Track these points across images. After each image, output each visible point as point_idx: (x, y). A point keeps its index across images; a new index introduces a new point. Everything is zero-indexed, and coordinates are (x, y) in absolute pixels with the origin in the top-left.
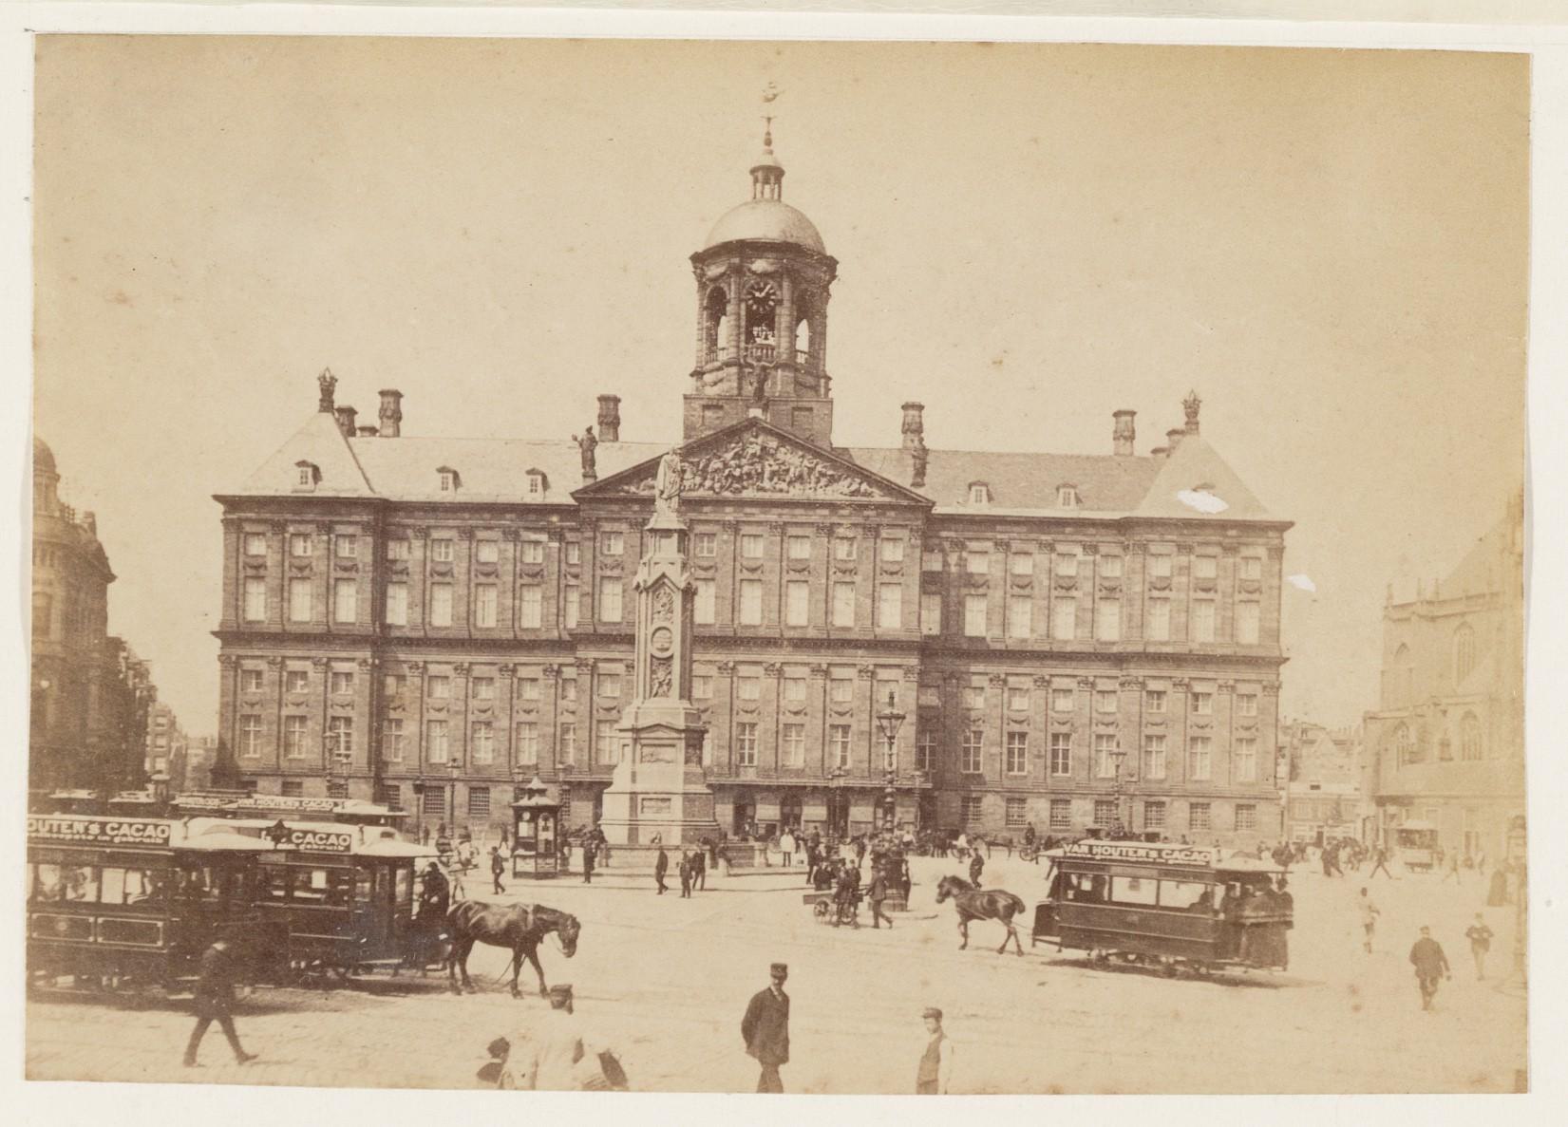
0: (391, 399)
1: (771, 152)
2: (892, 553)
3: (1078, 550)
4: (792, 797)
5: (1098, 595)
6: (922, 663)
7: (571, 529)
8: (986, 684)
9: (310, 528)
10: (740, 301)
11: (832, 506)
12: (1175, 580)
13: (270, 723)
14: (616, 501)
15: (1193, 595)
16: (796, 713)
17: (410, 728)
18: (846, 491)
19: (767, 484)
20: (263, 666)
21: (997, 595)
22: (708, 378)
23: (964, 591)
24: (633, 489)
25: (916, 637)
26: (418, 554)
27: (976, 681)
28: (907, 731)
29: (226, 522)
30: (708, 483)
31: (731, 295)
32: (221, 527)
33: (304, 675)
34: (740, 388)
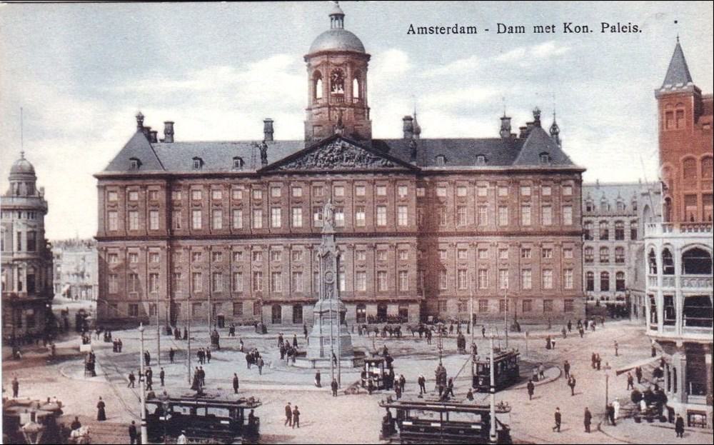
0: (170, 125)
1: (338, 6)
2: (403, 192)
3: (487, 184)
4: (361, 304)
6: (418, 241)
7: (255, 184)
8: (447, 247)
9: (137, 187)
10: (328, 76)
11: (375, 172)
12: (533, 197)
13: (121, 278)
14: (276, 174)
16: (362, 266)
17: (184, 277)
18: (380, 164)
19: (344, 163)
20: (117, 251)
22: (314, 111)
24: (284, 167)
26: (186, 197)
28: (413, 272)
29: (99, 187)
30: (318, 164)
31: (323, 74)
32: (96, 190)
33: (136, 254)
34: (329, 116)
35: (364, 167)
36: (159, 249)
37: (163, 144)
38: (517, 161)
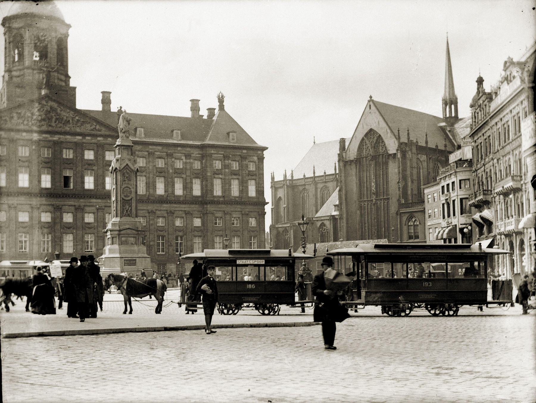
3: (183, 158)
11: (84, 135)
22: (14, 73)
30: (25, 122)
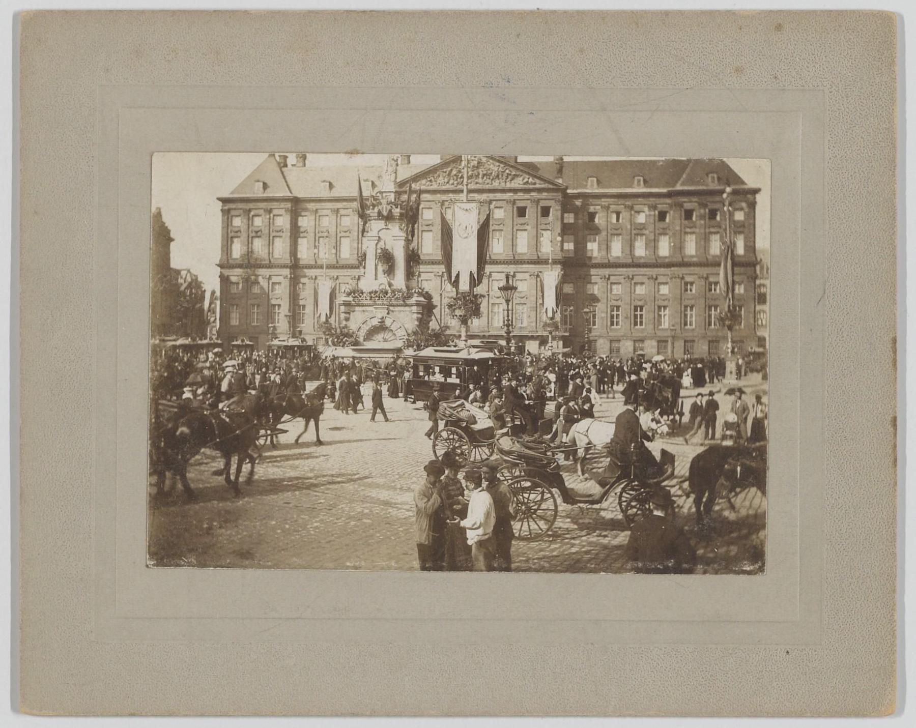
3: (646, 209)
5: (657, 232)
8: (599, 280)
11: (515, 191)
15: (707, 230)
19: (480, 180)
21: (604, 233)
23: (587, 232)
25: (559, 256)
27: (594, 279)
30: (451, 182)
32: (220, 214)
35: (503, 184)
36: (281, 278)
37: (294, 168)
38: (680, 182)
